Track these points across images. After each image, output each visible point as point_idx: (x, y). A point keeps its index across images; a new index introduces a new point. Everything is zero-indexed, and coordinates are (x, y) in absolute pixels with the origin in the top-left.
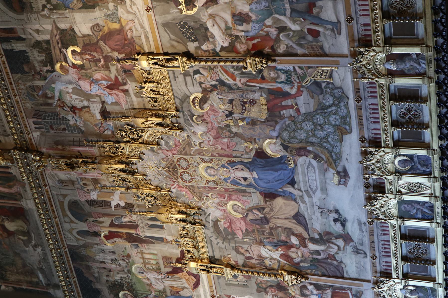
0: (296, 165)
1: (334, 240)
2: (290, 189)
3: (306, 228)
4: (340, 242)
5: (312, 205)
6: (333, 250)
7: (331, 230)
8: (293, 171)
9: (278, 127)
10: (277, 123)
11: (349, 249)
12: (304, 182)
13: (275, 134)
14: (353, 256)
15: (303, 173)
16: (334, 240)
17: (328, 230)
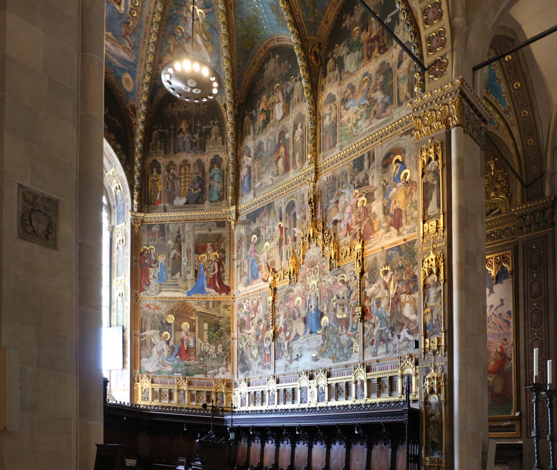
0: (319, 334)
1: (290, 355)
2: (308, 331)
3: (293, 340)
4: (289, 358)
5: (303, 343)
6: (286, 354)
7: (294, 353)
8: (316, 333)
9: (334, 324)
10: (335, 323)
11: (287, 363)
12: (312, 339)
13: (331, 323)
14: (284, 365)
15: (315, 338)
16: (290, 355)
17: (294, 351)
